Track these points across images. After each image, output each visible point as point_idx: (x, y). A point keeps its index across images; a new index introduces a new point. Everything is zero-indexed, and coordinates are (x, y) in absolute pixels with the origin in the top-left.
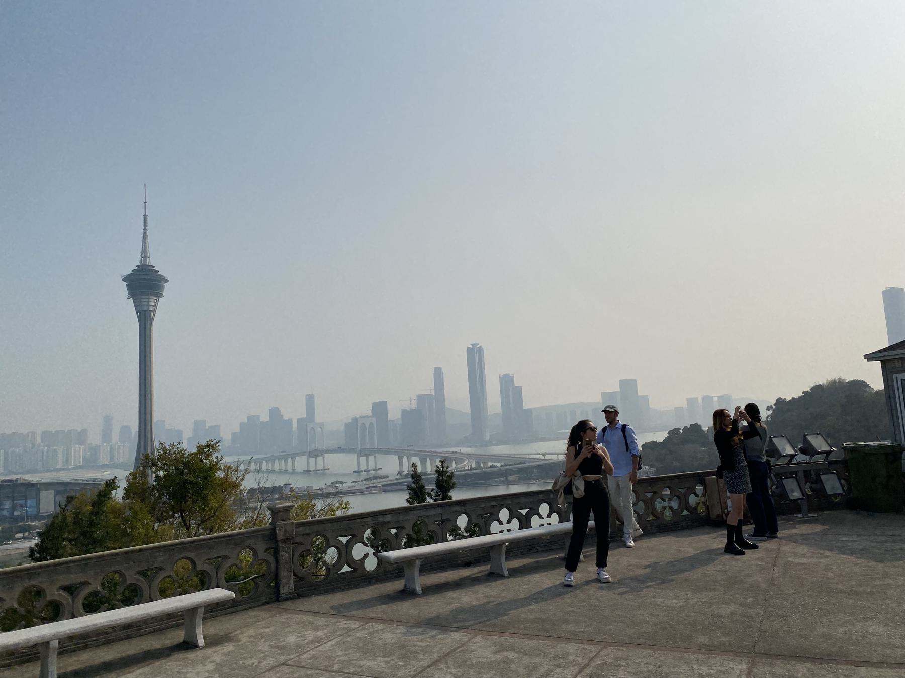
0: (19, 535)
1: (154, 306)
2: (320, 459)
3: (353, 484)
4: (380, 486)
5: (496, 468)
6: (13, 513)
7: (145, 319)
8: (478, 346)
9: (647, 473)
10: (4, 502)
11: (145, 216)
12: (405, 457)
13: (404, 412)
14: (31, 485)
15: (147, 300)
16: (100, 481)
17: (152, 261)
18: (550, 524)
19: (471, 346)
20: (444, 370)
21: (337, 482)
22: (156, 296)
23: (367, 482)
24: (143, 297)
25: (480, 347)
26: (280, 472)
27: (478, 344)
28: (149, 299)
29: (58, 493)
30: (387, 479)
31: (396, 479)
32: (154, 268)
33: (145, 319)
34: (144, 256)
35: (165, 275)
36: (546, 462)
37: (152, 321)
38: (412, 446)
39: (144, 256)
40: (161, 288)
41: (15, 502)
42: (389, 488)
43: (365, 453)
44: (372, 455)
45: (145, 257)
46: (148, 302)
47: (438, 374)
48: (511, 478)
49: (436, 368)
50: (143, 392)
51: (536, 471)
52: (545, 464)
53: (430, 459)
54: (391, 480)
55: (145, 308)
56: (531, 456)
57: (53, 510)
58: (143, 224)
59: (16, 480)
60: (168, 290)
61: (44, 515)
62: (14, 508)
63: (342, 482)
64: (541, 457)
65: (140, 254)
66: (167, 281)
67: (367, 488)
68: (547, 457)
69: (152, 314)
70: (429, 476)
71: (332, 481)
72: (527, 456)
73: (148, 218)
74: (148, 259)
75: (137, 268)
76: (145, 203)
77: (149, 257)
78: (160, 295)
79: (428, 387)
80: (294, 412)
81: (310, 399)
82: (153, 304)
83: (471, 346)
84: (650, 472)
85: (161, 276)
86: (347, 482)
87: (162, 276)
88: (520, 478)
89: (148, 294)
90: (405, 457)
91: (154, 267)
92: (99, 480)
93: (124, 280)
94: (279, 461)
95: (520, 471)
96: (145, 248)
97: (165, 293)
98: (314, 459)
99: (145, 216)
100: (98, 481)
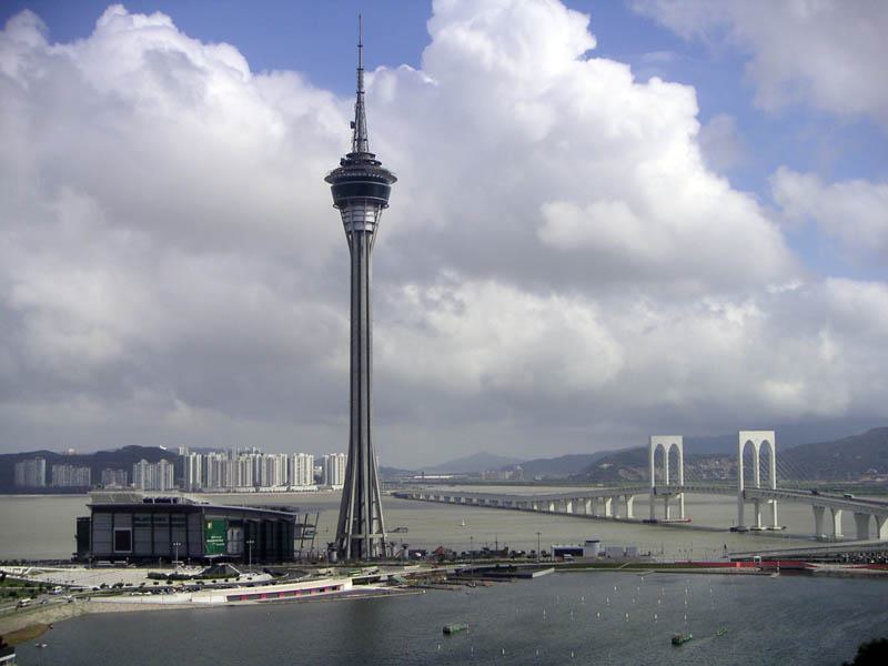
4: (757, 560)
14: (190, 509)
15: (361, 213)
34: (359, 139)
39: (359, 139)
40: (385, 192)
59: (175, 500)
66: (395, 179)
78: (383, 205)
93: (327, 179)
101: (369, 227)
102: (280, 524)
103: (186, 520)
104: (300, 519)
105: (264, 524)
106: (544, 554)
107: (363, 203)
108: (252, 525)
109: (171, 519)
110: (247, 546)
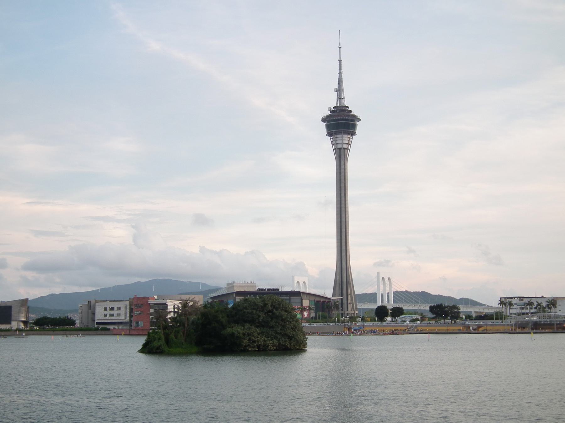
11: (340, 61)
15: (341, 138)
18: (559, 310)
22: (349, 134)
24: (338, 136)
34: (340, 99)
39: (340, 99)
40: (354, 126)
46: (342, 140)
66: (359, 120)
73: (343, 63)
74: (343, 101)
76: (340, 48)
78: (353, 134)
89: (342, 133)
93: (324, 120)
97: (358, 130)
99: (340, 61)
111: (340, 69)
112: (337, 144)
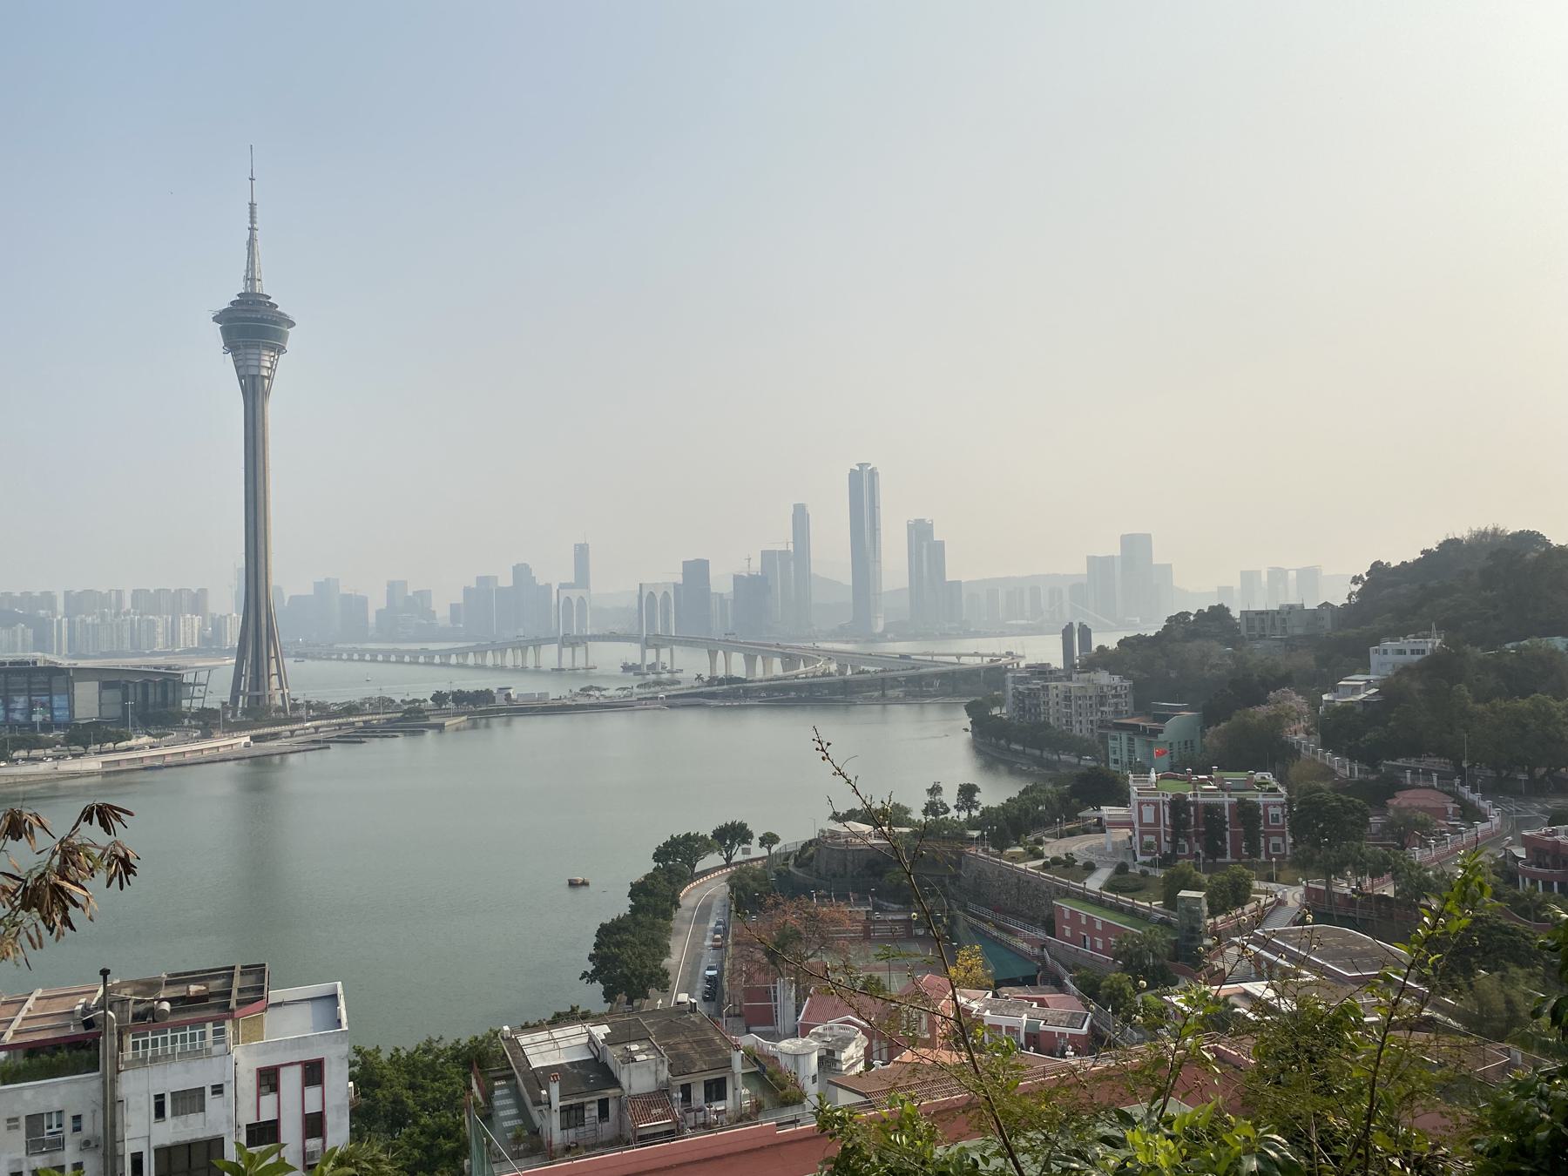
0: (23, 753)
1: (269, 368)
2: (580, 651)
3: (620, 692)
4: (662, 698)
5: (866, 675)
6: (31, 719)
7: (254, 390)
8: (869, 468)
9: (1116, 688)
10: (16, 698)
11: (252, 205)
12: (720, 653)
13: (737, 579)
14: (54, 671)
16: (178, 670)
17: (264, 287)
19: (857, 468)
20: (809, 510)
21: (591, 688)
22: (273, 349)
23: (642, 690)
25: (873, 469)
26: (496, 668)
27: (869, 464)
28: (260, 354)
29: (105, 686)
30: (679, 687)
31: (692, 687)
32: (270, 301)
33: (254, 390)
34: (251, 279)
35: (286, 312)
36: (961, 667)
37: (266, 394)
38: (734, 634)
39: (251, 279)
40: (282, 336)
41: (33, 698)
42: (679, 701)
43: (654, 642)
44: (662, 647)
45: (253, 280)
46: (259, 360)
47: (800, 517)
48: (890, 693)
49: (796, 507)
50: (251, 518)
51: (937, 683)
52: (954, 672)
53: (762, 657)
54: (683, 689)
55: (253, 371)
56: (935, 658)
57: (98, 715)
58: (249, 219)
60: (294, 338)
61: (81, 722)
62: (30, 711)
63: (598, 689)
64: (954, 659)
65: (244, 274)
66: (292, 324)
67: (639, 699)
68: (964, 660)
69: (267, 381)
70: (748, 685)
71: (583, 687)
72: (929, 658)
73: (258, 210)
75: (238, 298)
77: (259, 280)
78: (280, 350)
79: (781, 538)
80: (554, 572)
81: (582, 552)
82: (269, 365)
83: (857, 468)
84: (1121, 686)
85: (280, 314)
86: (608, 689)
87: (286, 315)
88: (907, 694)
90: (720, 653)
91: (270, 298)
92: (177, 667)
93: (216, 319)
94: (493, 653)
95: (910, 680)
96: (253, 262)
97: (290, 345)
98: (571, 649)
99: (252, 205)
100: (175, 670)
101: (265, 373)
102: (164, 684)
103: (49, 682)
104: (189, 678)
105: (145, 685)
106: (295, 707)
107: (257, 346)
108: (130, 685)
109: (30, 683)
110: (125, 708)
111: (252, 221)
112: (248, 366)
